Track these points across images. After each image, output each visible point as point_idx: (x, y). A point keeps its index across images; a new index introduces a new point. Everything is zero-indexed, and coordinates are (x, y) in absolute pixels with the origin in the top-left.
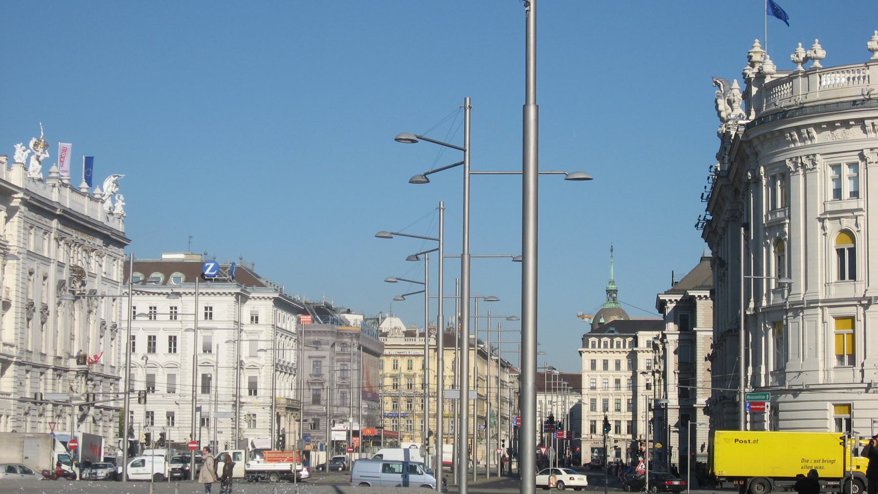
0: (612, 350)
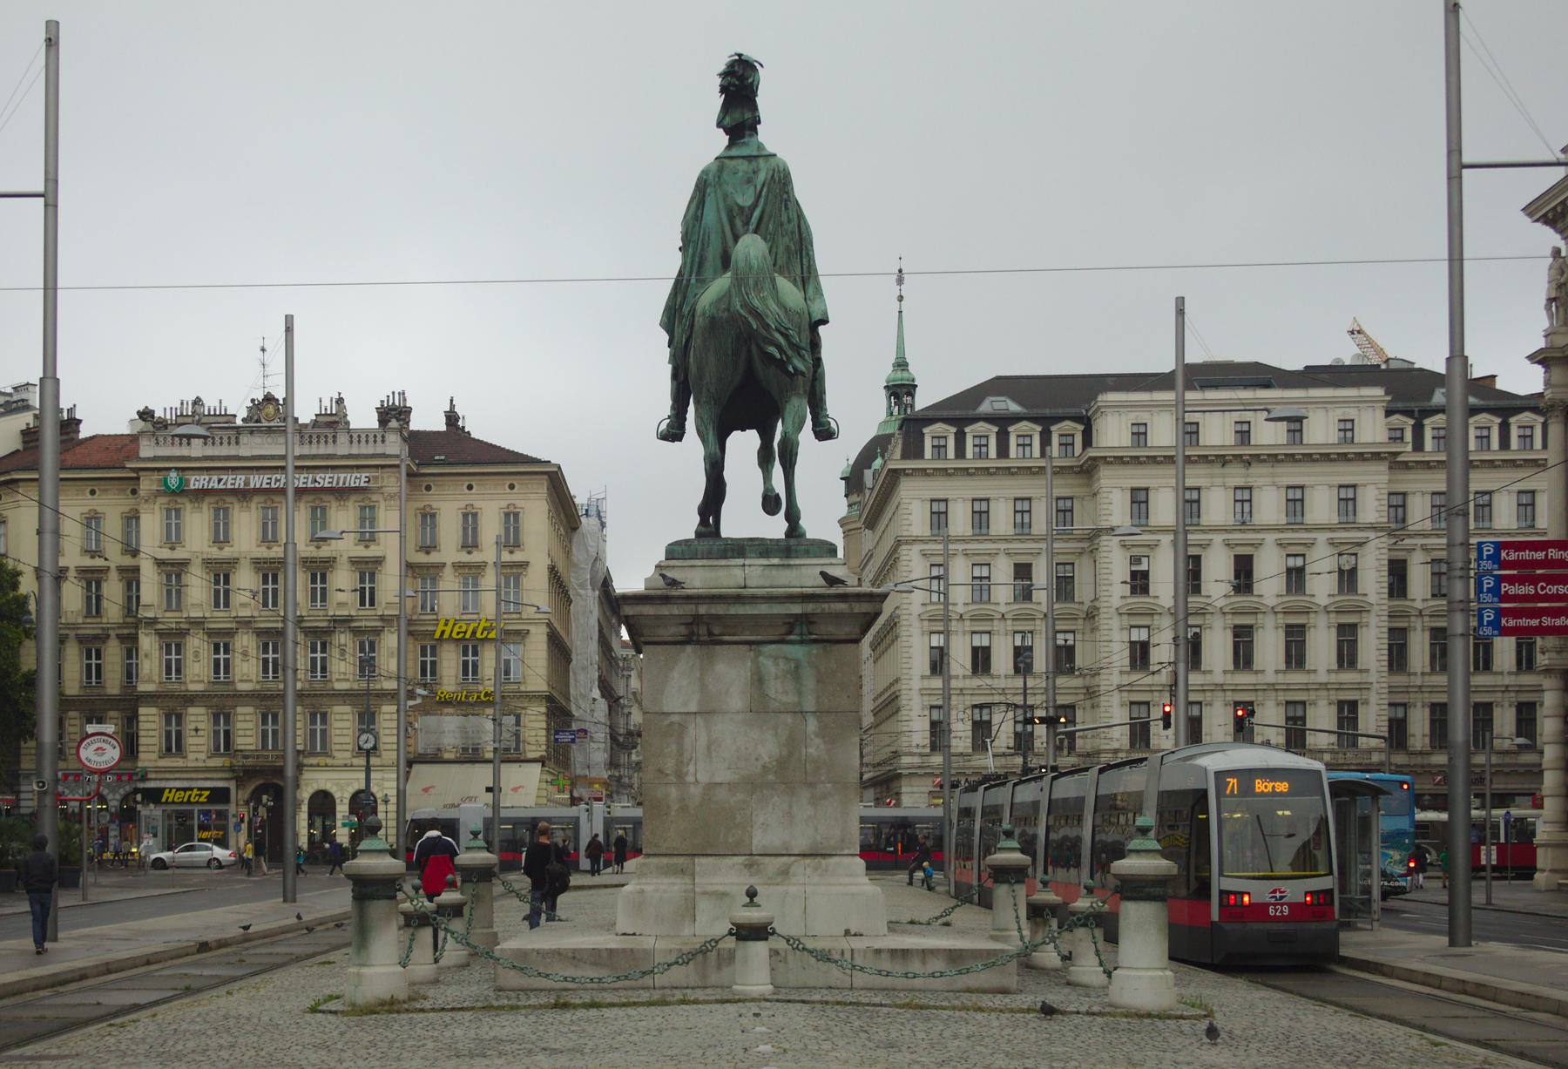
0: (1003, 463)
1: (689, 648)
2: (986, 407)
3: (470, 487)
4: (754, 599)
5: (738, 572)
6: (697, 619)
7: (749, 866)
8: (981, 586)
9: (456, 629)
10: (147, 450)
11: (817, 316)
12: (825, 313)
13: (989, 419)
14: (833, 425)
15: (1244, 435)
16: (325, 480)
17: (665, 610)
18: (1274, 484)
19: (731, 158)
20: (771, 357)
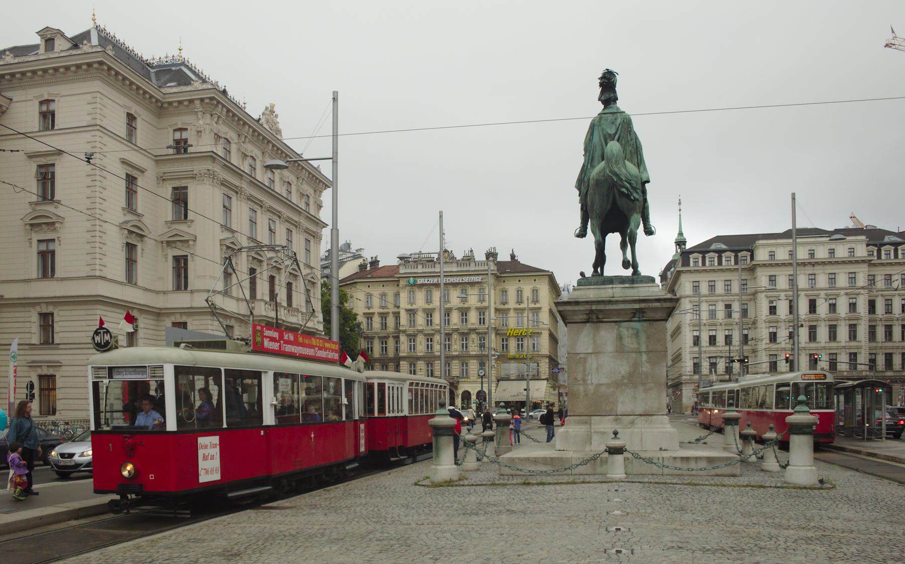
0: (720, 267)
1: (588, 325)
2: (713, 247)
3: (519, 281)
4: (617, 302)
5: (610, 291)
6: (591, 311)
7: (616, 420)
8: (713, 314)
9: (515, 332)
10: (402, 270)
11: (644, 179)
12: (648, 178)
13: (715, 251)
14: (653, 229)
15: (812, 255)
16: (466, 279)
17: (577, 308)
18: (824, 273)
19: (605, 114)
20: (623, 193)
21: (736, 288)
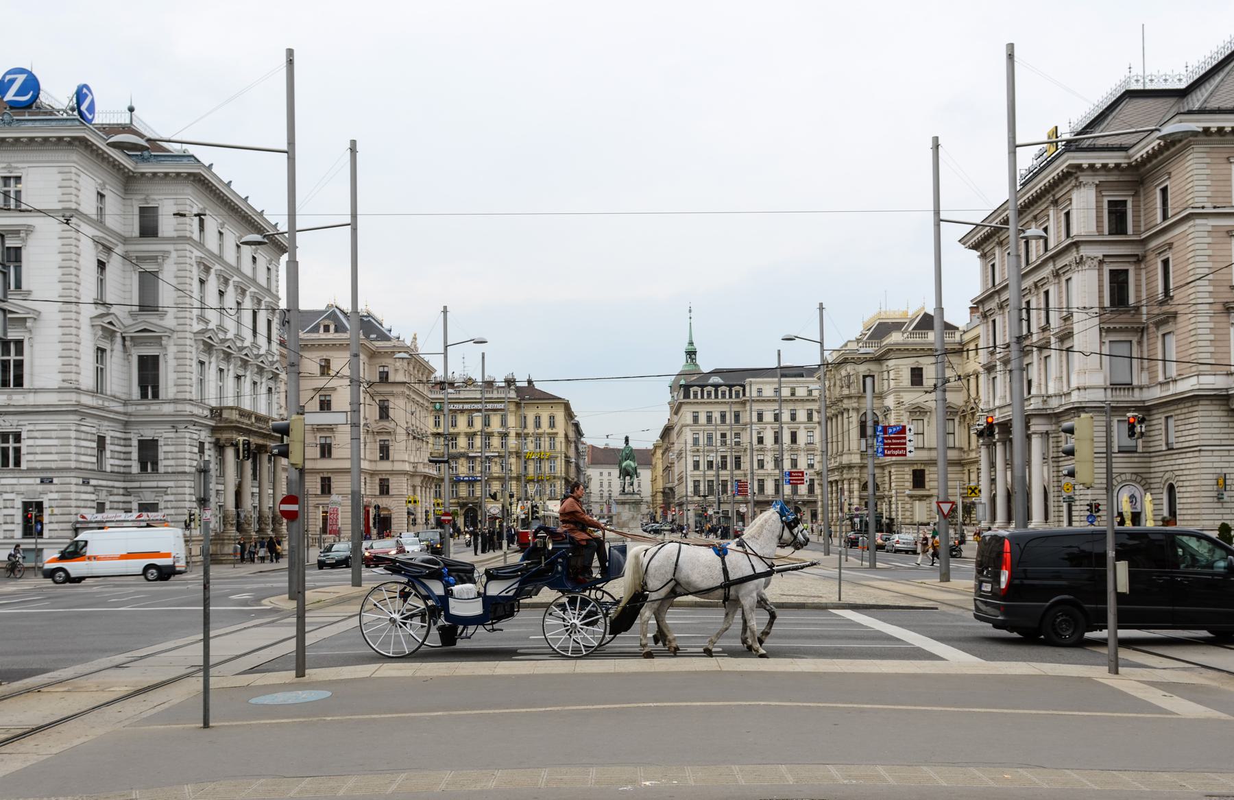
16: (489, 406)
21: (730, 418)
